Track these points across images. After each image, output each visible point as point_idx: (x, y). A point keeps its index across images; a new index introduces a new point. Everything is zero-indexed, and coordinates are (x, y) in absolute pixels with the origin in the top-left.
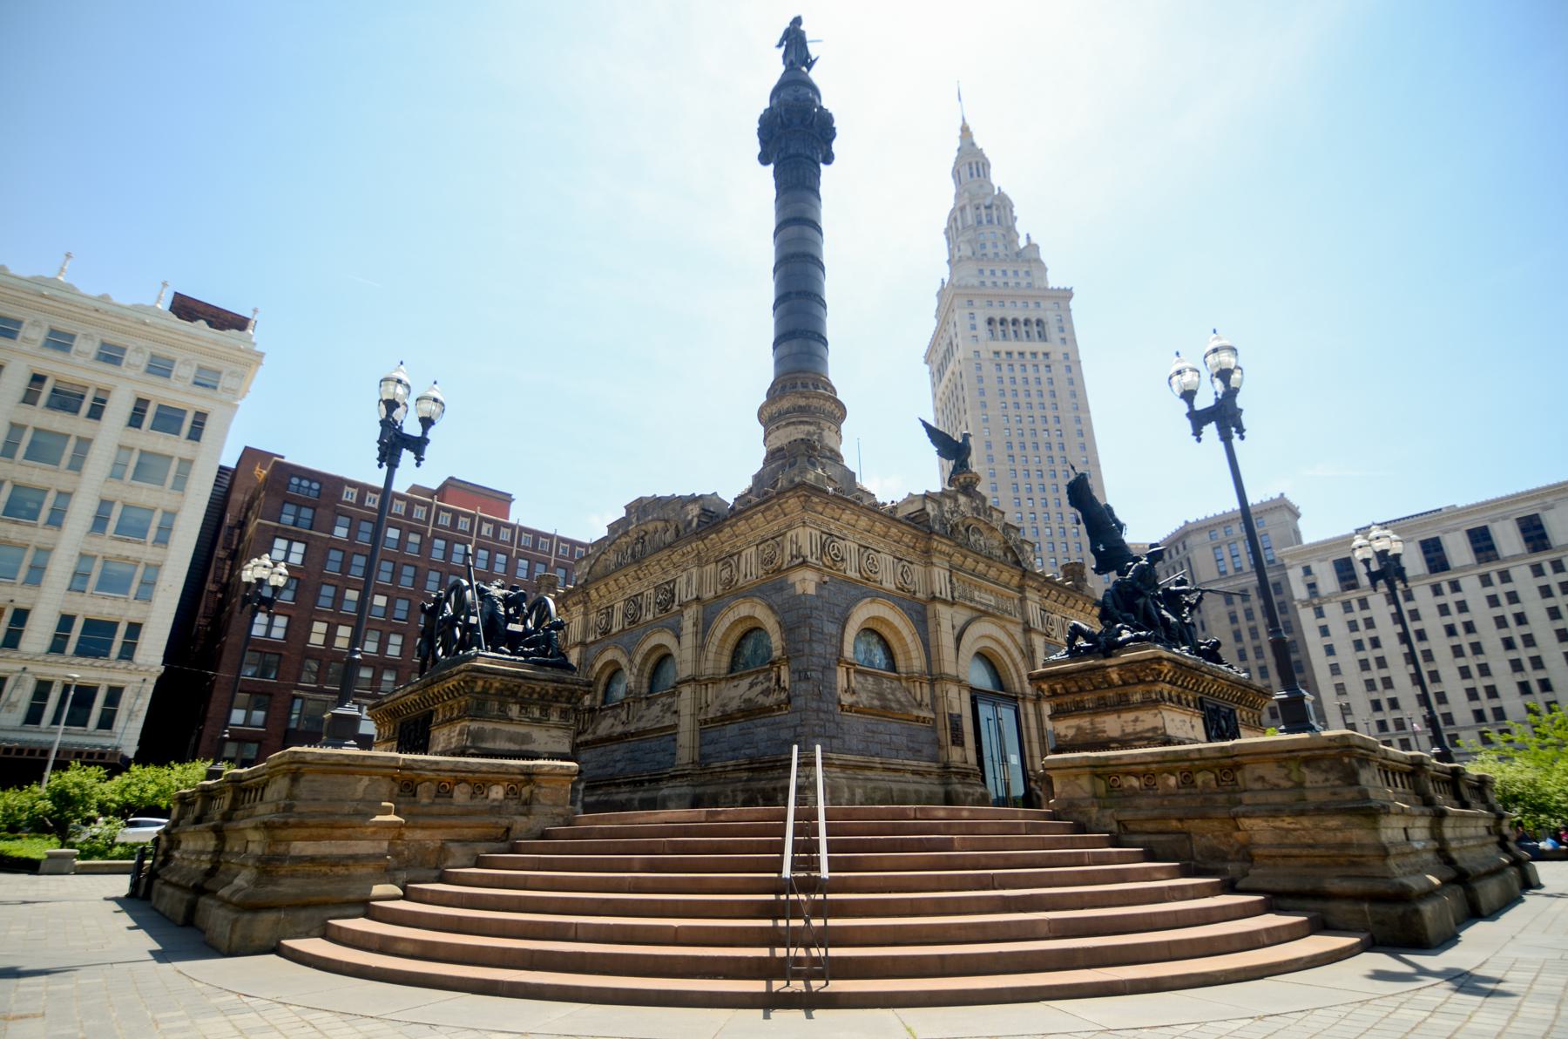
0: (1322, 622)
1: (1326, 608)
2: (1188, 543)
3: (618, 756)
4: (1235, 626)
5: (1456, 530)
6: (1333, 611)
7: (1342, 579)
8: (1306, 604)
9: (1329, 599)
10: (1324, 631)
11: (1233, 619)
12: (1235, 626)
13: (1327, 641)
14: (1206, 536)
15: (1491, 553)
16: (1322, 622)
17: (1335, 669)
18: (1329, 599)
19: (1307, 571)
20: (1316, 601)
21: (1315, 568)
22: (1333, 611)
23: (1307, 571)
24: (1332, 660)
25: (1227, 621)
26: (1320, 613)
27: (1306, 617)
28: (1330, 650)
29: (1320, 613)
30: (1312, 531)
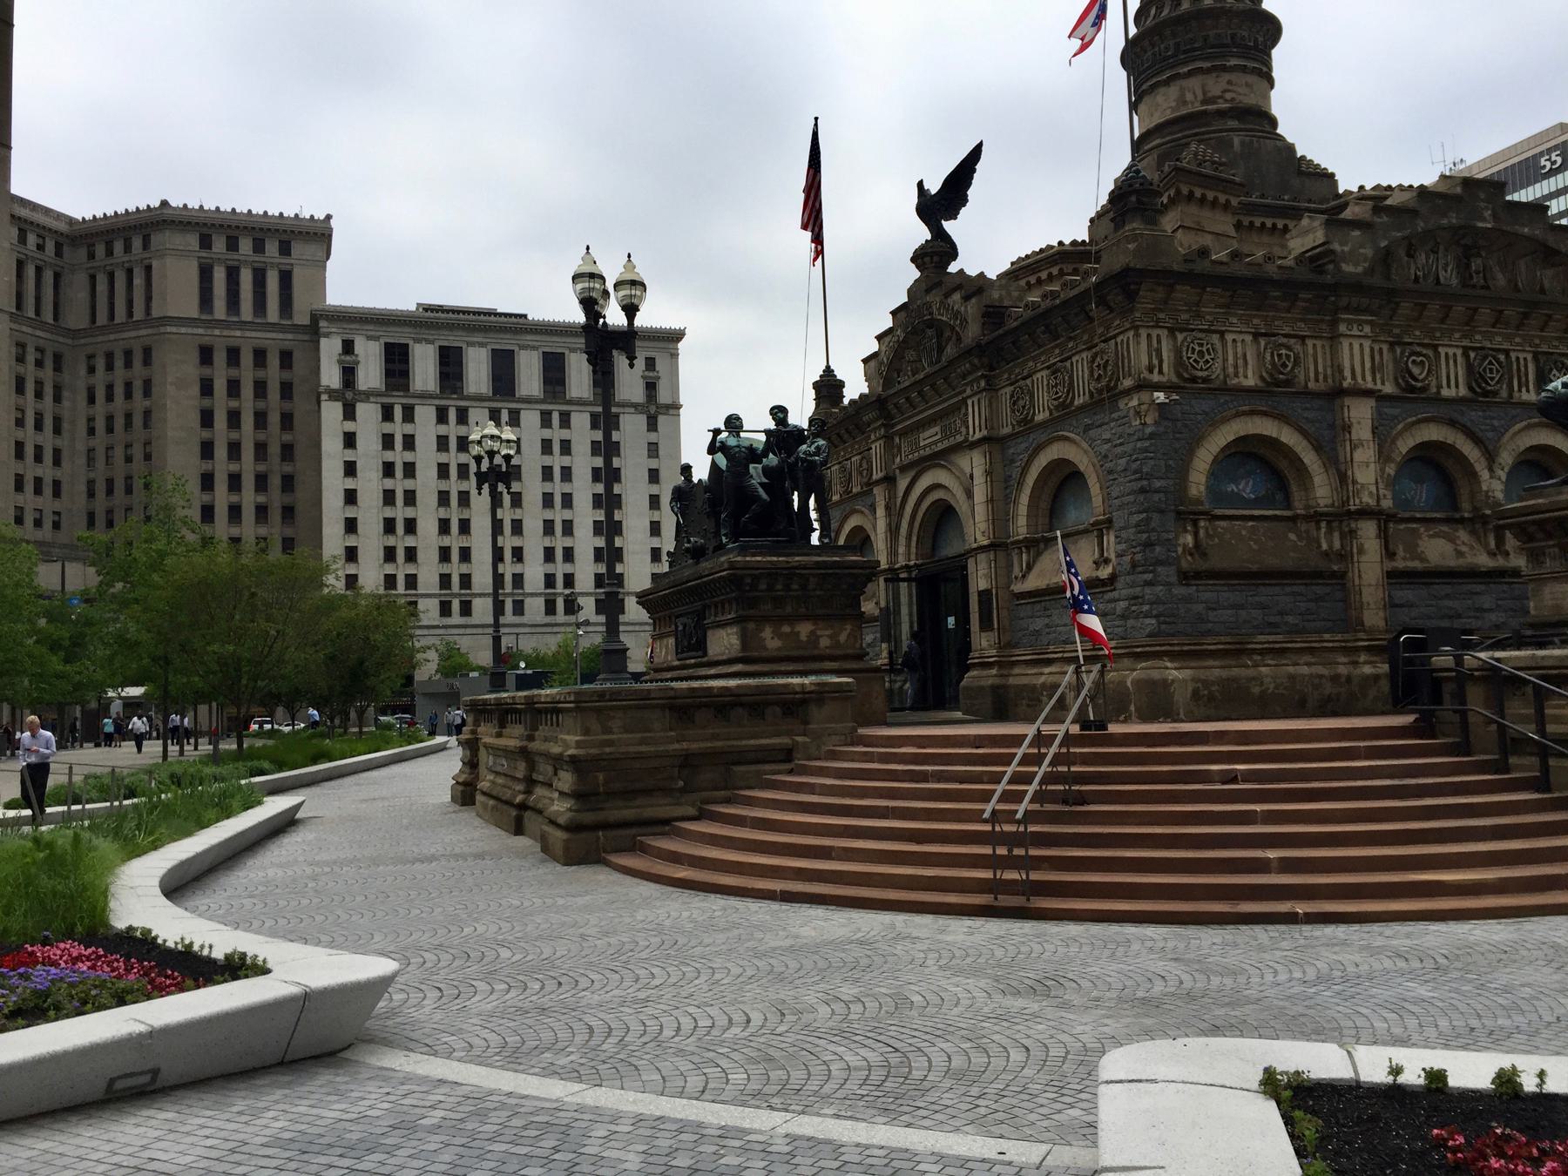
0: (349, 426)
1: (361, 409)
2: (156, 239)
3: (1487, 601)
4: (207, 402)
5: (534, 348)
6: (368, 413)
7: (389, 373)
8: (334, 395)
9: (367, 396)
10: (350, 440)
11: (207, 388)
12: (207, 402)
13: (350, 455)
14: (193, 241)
15: (558, 388)
16: (349, 426)
17: (351, 497)
18: (367, 396)
19: (348, 347)
20: (349, 395)
21: (360, 345)
22: (368, 413)
23: (348, 347)
24: (350, 484)
25: (195, 390)
26: (350, 414)
27: (331, 412)
28: (350, 469)
29: (350, 414)
30: (348, 283)
